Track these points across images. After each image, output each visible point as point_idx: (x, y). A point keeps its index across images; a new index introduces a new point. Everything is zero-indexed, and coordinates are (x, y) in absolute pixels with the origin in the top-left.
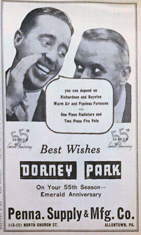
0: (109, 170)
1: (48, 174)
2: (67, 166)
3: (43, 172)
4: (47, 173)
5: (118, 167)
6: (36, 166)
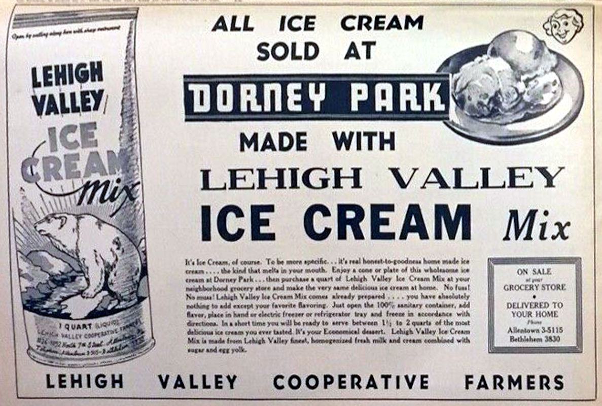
2: (312, 87)
3: (249, 103)
4: (258, 104)
6: (229, 88)
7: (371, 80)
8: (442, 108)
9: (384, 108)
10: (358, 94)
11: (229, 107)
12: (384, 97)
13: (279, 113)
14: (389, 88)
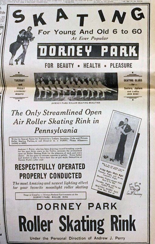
0: (125, 51)
1: (66, 54)
2: (86, 47)
3: (62, 53)
5: (134, 49)
7: (109, 45)
8: (136, 55)
9: (114, 55)
10: (105, 49)
11: (54, 54)
12: (114, 51)
13: (73, 56)
14: (116, 48)
